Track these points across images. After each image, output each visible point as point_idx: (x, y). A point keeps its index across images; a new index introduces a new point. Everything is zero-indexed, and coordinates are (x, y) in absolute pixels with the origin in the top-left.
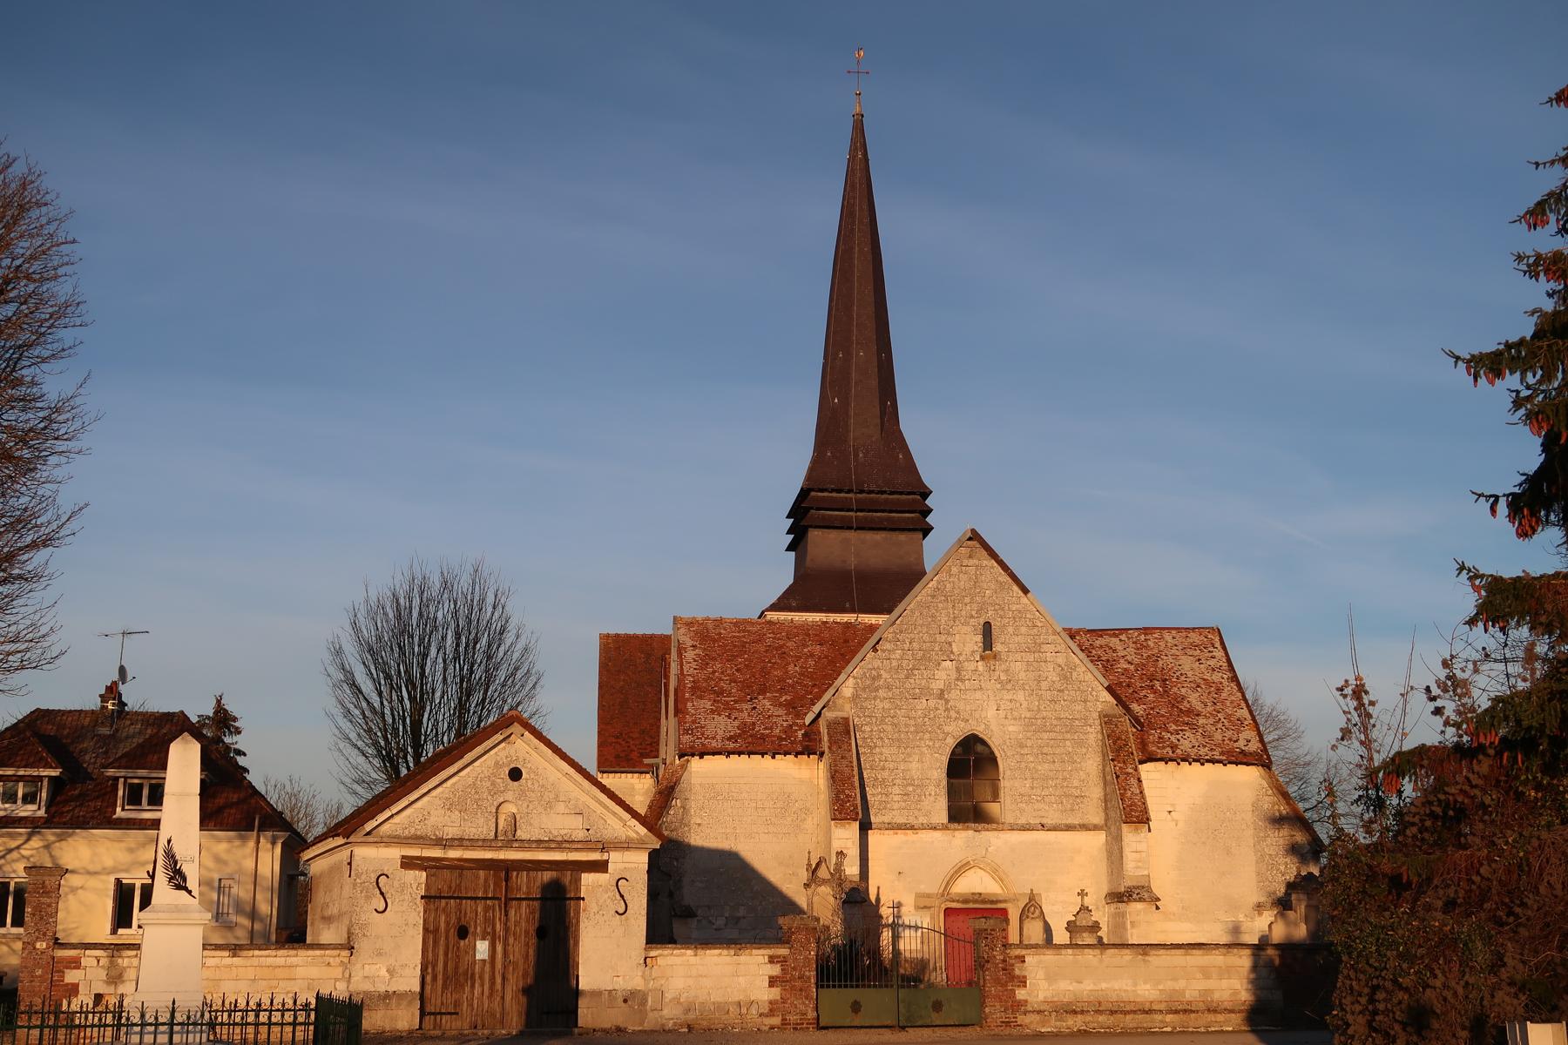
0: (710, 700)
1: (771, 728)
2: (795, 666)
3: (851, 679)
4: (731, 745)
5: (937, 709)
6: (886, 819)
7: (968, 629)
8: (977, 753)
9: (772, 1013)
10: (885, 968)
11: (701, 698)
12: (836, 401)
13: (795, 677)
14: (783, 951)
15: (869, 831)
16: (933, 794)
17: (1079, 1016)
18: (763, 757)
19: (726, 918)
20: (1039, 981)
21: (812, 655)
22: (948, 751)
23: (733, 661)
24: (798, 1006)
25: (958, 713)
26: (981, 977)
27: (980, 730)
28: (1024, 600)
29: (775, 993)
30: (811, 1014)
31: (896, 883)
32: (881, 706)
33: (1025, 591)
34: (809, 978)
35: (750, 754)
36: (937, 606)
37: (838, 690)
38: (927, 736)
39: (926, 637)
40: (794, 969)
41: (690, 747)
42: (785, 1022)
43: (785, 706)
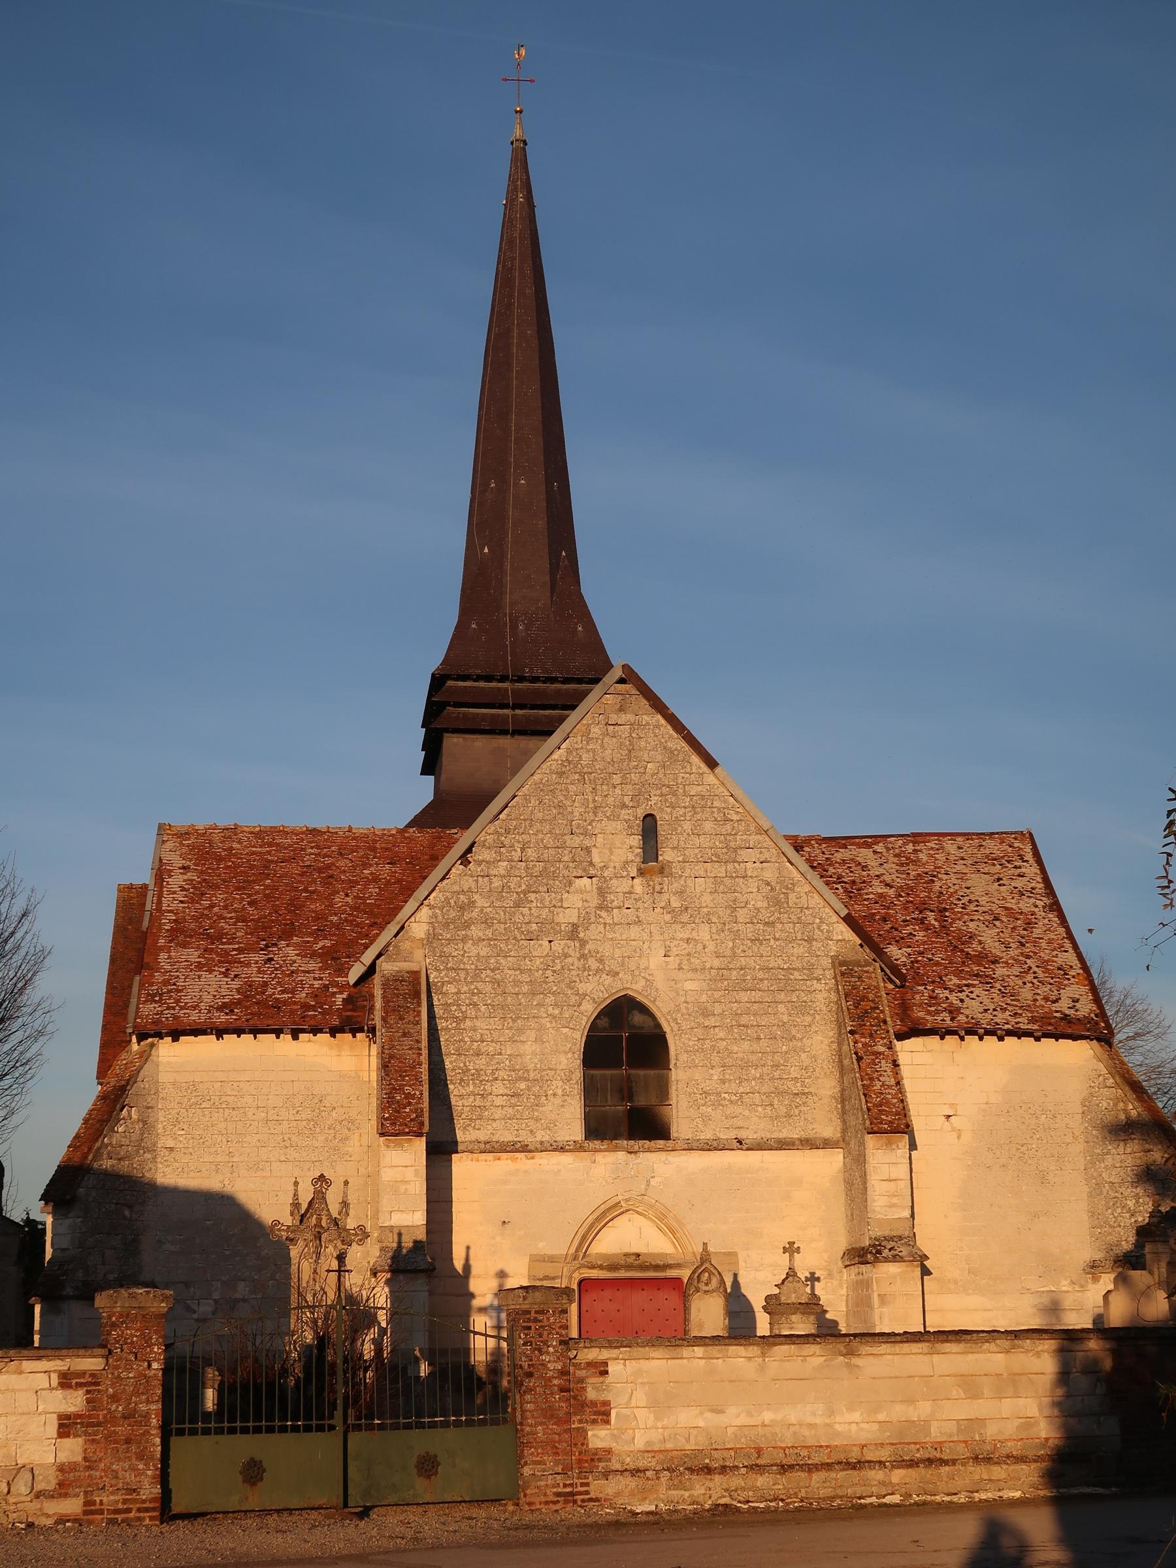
0: (198, 948)
1: (293, 991)
2: (347, 895)
3: (425, 910)
4: (222, 1018)
5: (566, 956)
6: (482, 1135)
7: (619, 825)
8: (634, 1027)
9: (62, 1489)
10: (479, 1379)
11: (185, 945)
12: (486, 550)
13: (344, 912)
14: (91, 1363)
15: (454, 1156)
16: (560, 1092)
17: (717, 1478)
18: (278, 1037)
19: (215, 1300)
20: (636, 1411)
21: (375, 879)
22: (585, 1023)
23: (244, 888)
24: (120, 1474)
25: (601, 961)
26: (518, 1406)
27: (636, 989)
28: (710, 778)
29: (72, 1449)
30: (150, 1490)
31: (498, 1239)
32: (474, 952)
33: (712, 764)
34: (147, 1416)
35: (255, 1032)
36: (567, 789)
37: (402, 928)
38: (550, 999)
39: (548, 840)
40: (115, 1398)
41: (153, 1023)
42: (90, 1507)
43: (320, 955)
